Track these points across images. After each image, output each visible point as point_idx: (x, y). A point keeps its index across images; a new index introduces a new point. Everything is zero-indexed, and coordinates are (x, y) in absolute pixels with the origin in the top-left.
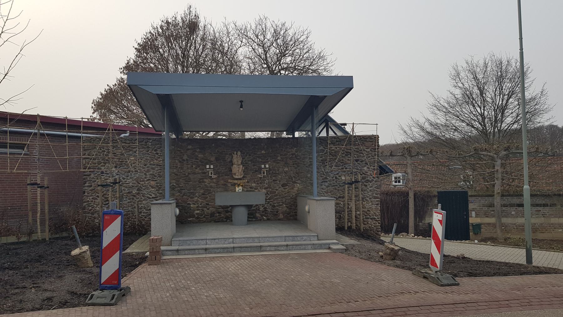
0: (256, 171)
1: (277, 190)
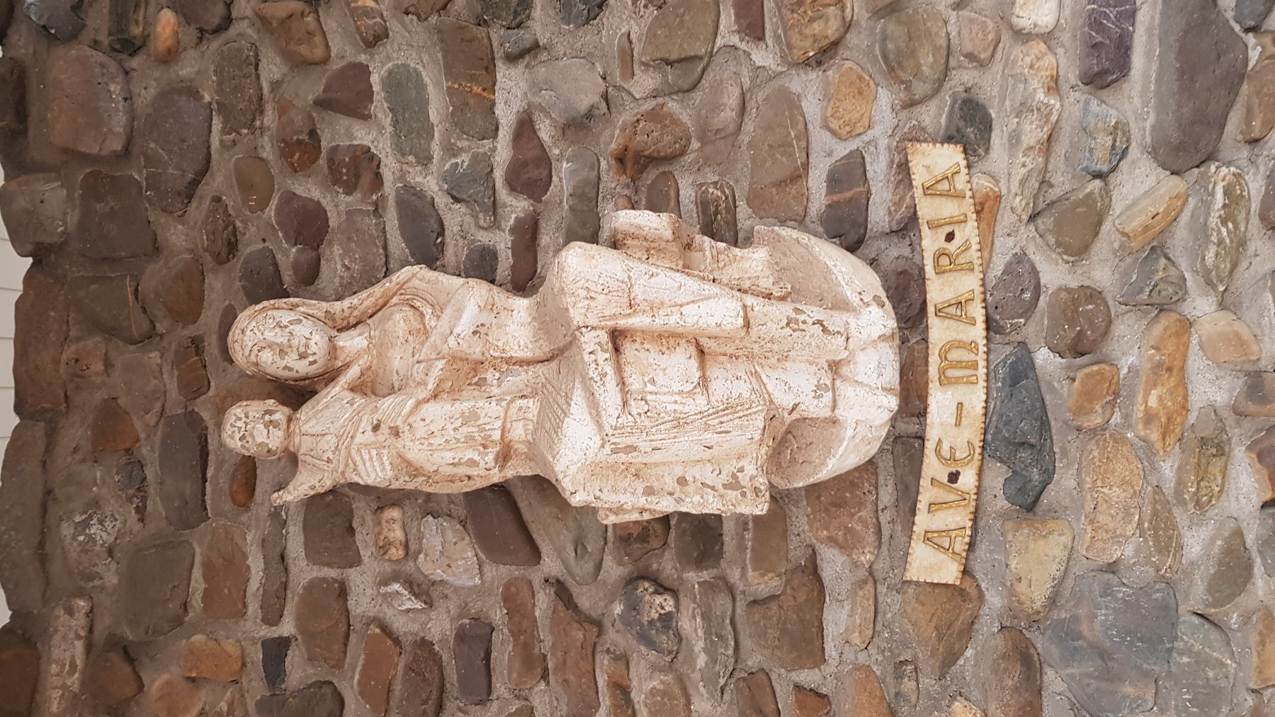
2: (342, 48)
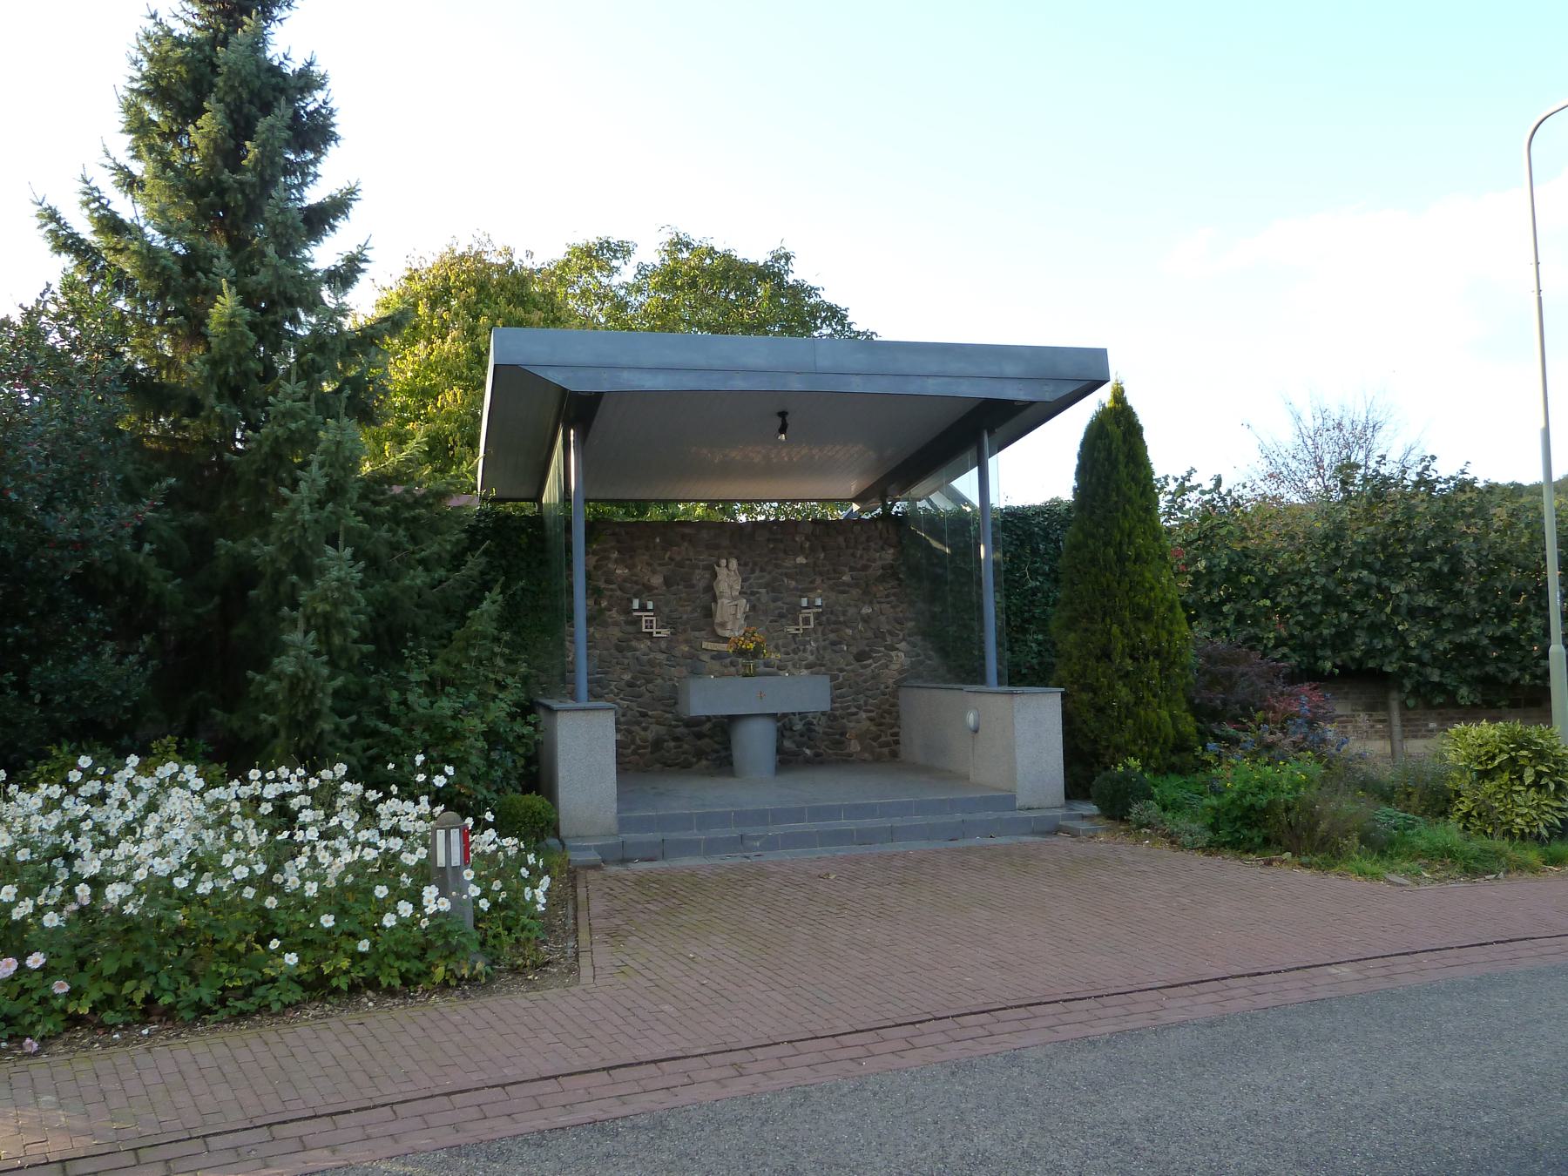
0: (781, 616)
1: (841, 670)
2: (770, 568)
